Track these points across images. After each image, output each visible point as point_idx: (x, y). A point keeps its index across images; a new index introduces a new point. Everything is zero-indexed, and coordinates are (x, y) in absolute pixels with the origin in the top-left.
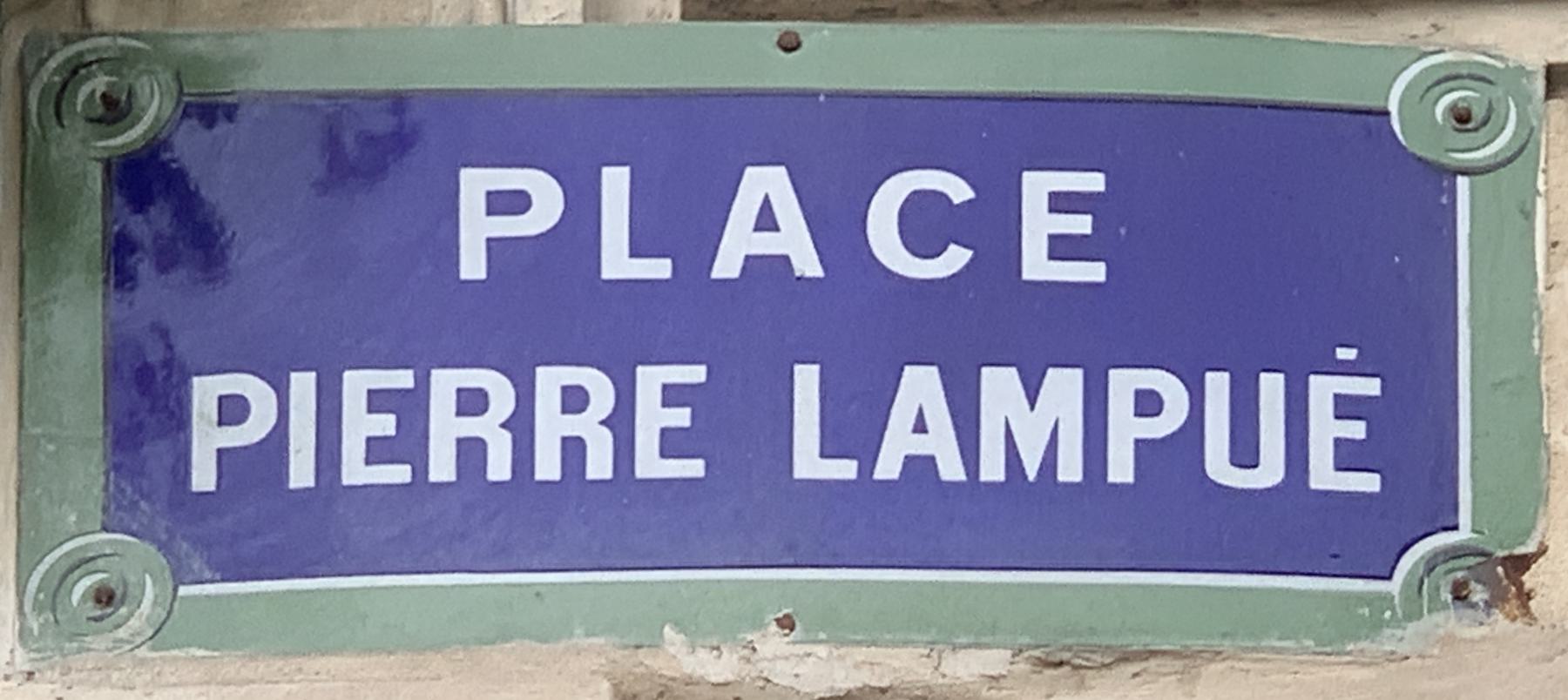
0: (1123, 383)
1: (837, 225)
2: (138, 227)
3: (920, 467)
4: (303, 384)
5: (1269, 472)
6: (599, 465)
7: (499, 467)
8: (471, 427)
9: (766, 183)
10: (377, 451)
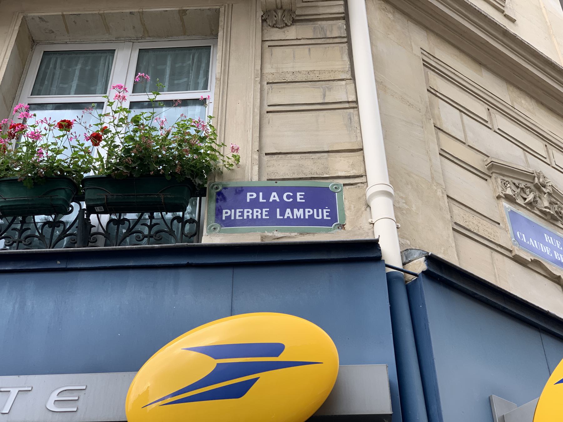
0: (307, 210)
1: (281, 197)
2: (219, 198)
3: (288, 217)
4: (233, 211)
5: (320, 217)
6: (259, 217)
7: (250, 217)
8: (248, 214)
9: (274, 194)
10: (239, 216)
